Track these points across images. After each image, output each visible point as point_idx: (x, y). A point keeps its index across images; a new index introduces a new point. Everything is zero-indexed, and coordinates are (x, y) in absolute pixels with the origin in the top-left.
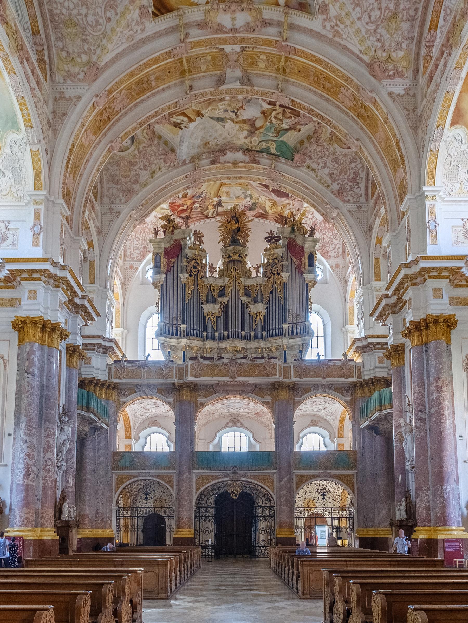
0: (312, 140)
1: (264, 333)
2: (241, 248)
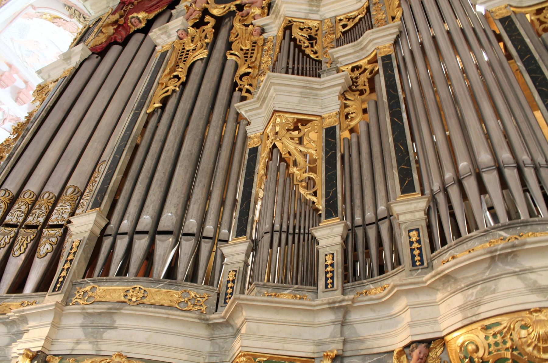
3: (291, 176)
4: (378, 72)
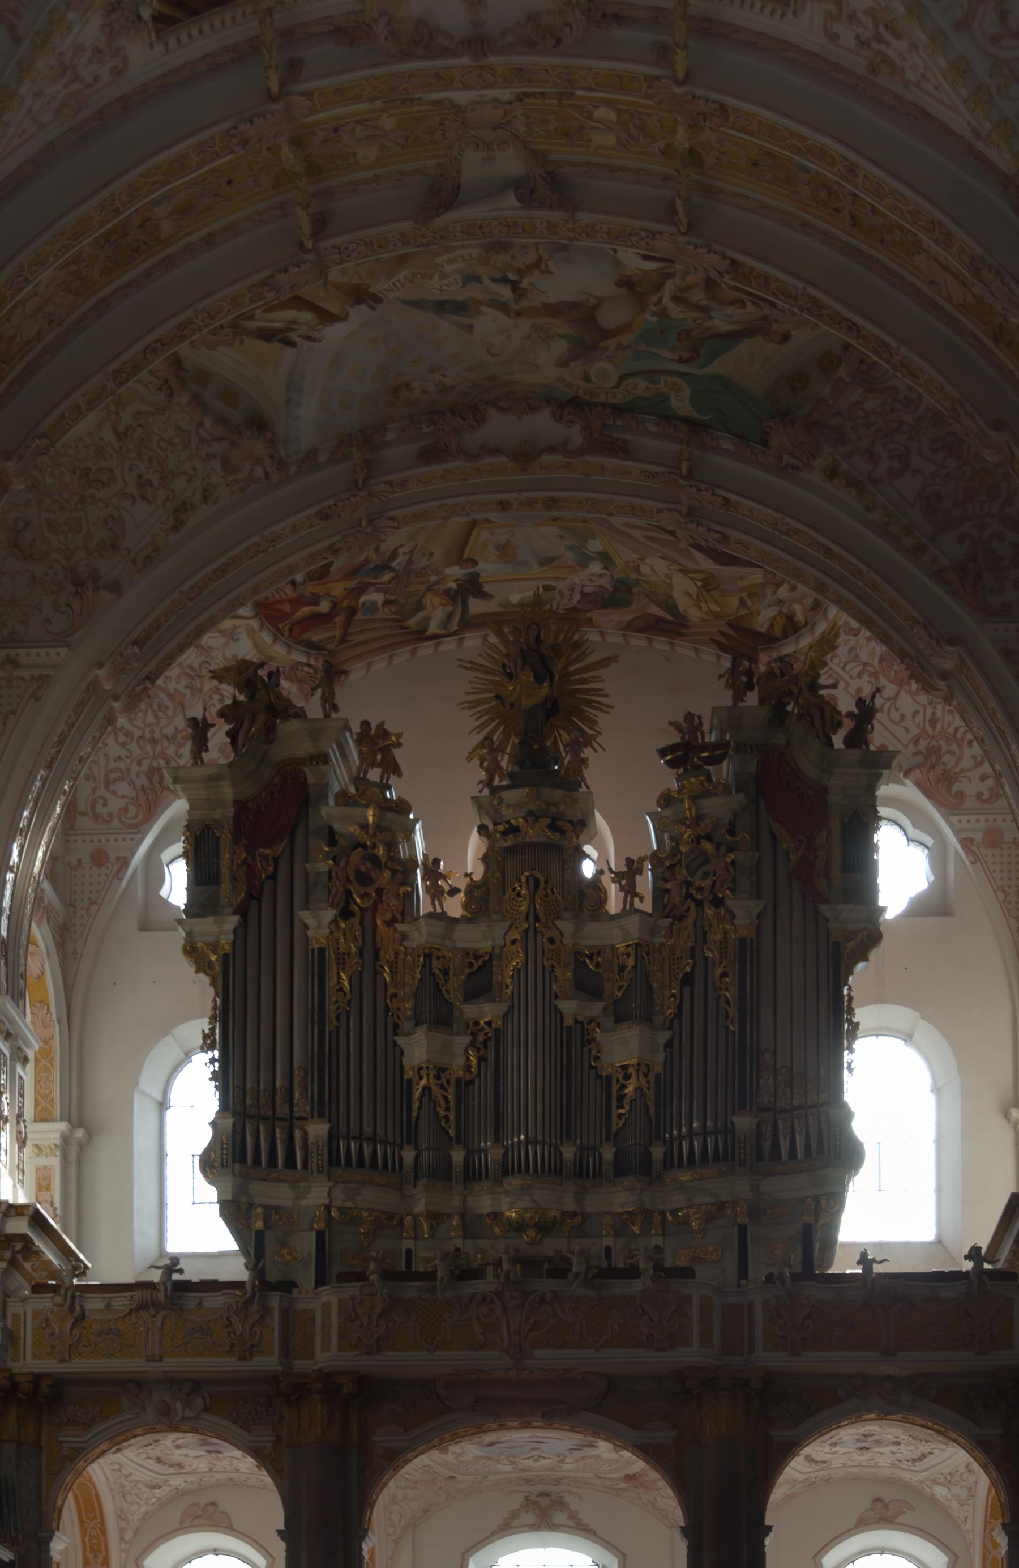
0: (842, 372)
1: (658, 1152)
2: (558, 793)
3: (438, 1113)
4: (490, 1038)
